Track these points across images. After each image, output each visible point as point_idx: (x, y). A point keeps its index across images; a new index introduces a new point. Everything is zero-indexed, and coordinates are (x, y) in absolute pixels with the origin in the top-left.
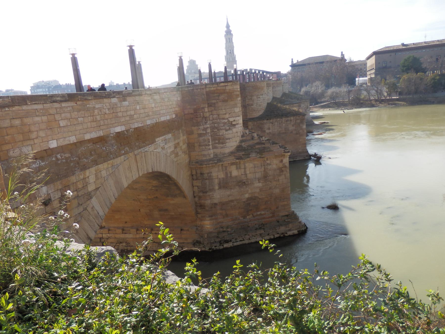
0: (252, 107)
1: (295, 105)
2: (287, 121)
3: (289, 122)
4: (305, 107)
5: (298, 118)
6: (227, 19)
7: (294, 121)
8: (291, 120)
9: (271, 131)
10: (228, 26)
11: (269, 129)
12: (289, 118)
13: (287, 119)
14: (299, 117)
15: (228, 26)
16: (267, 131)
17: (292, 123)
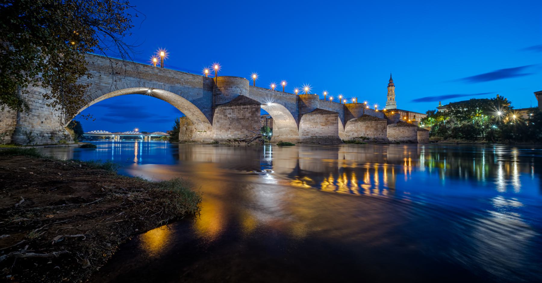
0: (220, 95)
1: (332, 115)
2: (244, 108)
3: (246, 110)
4: (382, 127)
5: (254, 106)
6: (391, 75)
7: (251, 109)
8: (248, 108)
9: (231, 116)
10: (391, 79)
11: (230, 114)
12: (246, 106)
13: (244, 107)
14: (255, 105)
15: (391, 79)
16: (229, 116)
17: (249, 111)
